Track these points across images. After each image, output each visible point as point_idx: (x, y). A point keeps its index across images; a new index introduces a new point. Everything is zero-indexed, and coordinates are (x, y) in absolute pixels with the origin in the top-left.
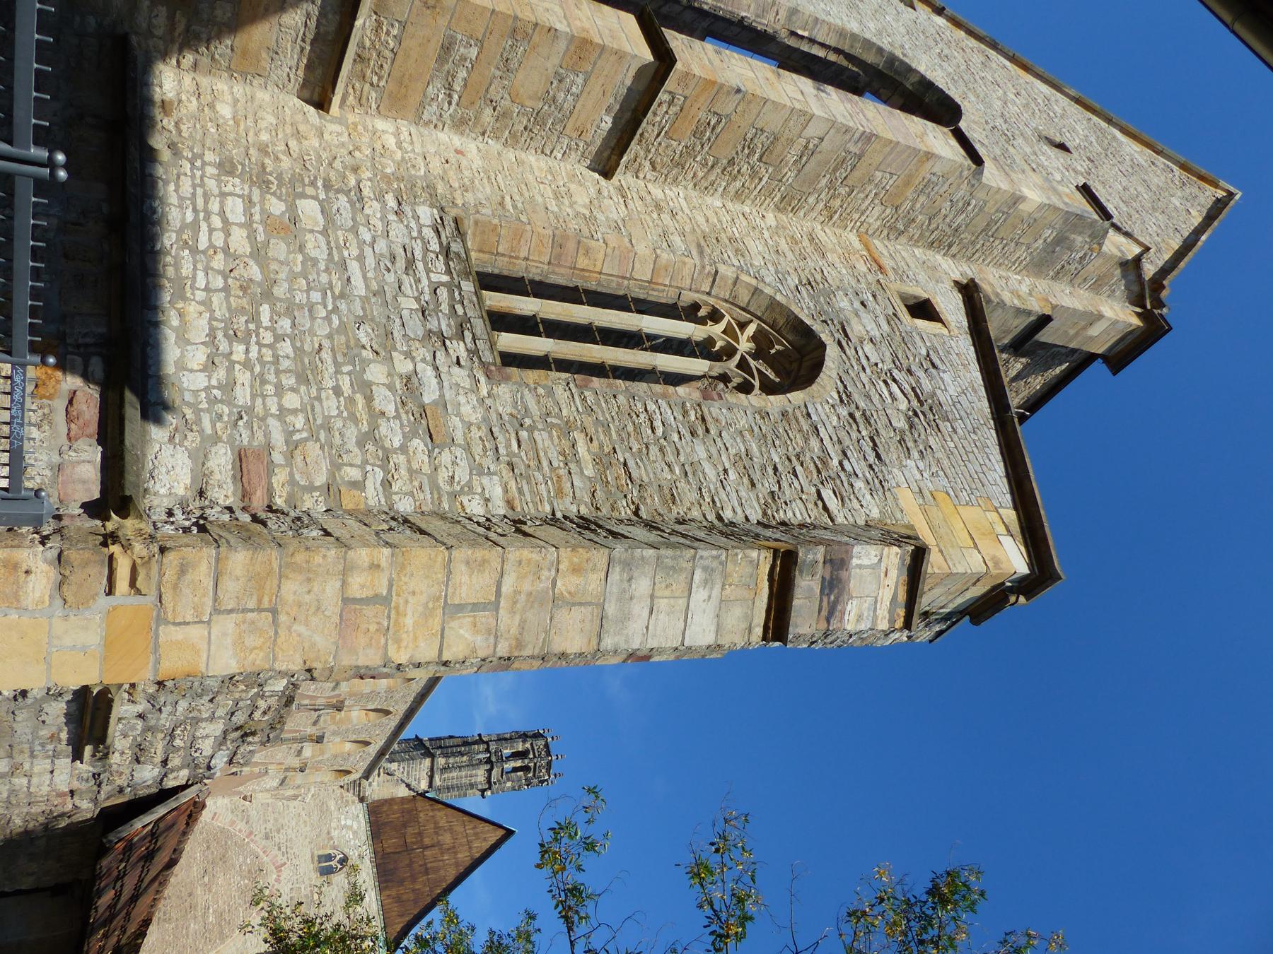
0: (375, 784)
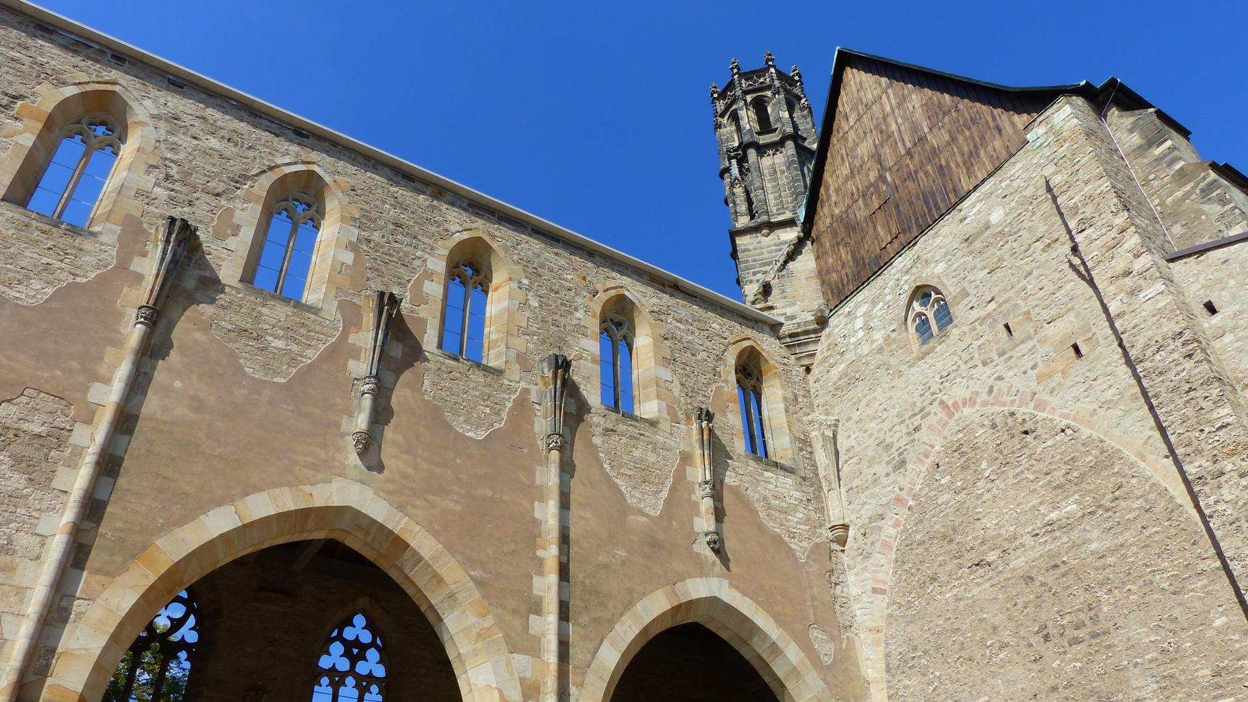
0: (789, 311)
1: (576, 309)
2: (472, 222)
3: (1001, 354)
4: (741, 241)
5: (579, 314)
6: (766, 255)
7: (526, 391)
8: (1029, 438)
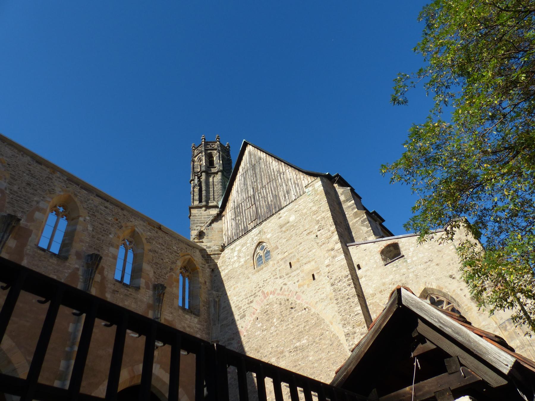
0: (208, 244)
1: (110, 234)
2: (67, 187)
3: (287, 275)
4: (194, 211)
5: (111, 236)
6: (203, 219)
7: (78, 269)
8: (293, 310)
